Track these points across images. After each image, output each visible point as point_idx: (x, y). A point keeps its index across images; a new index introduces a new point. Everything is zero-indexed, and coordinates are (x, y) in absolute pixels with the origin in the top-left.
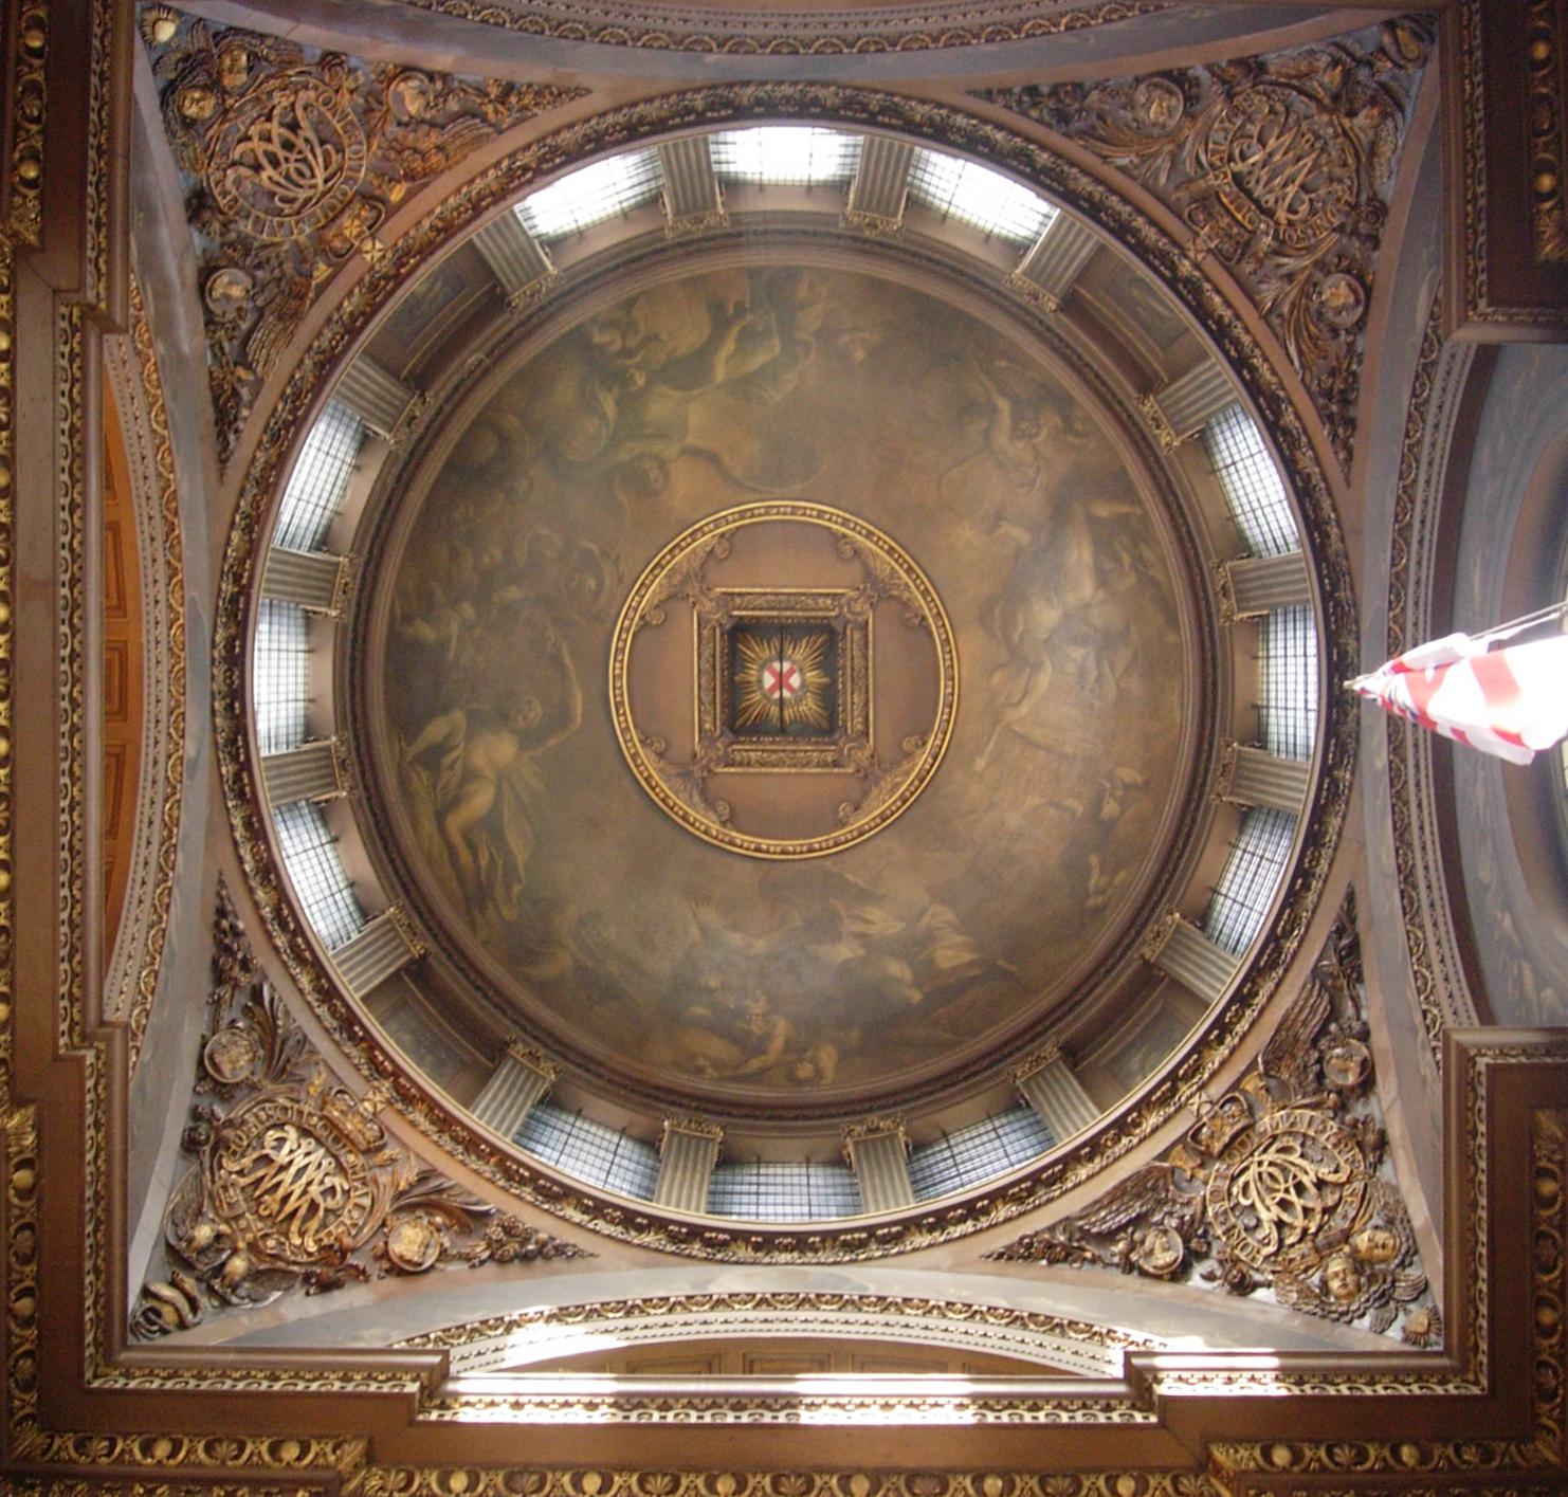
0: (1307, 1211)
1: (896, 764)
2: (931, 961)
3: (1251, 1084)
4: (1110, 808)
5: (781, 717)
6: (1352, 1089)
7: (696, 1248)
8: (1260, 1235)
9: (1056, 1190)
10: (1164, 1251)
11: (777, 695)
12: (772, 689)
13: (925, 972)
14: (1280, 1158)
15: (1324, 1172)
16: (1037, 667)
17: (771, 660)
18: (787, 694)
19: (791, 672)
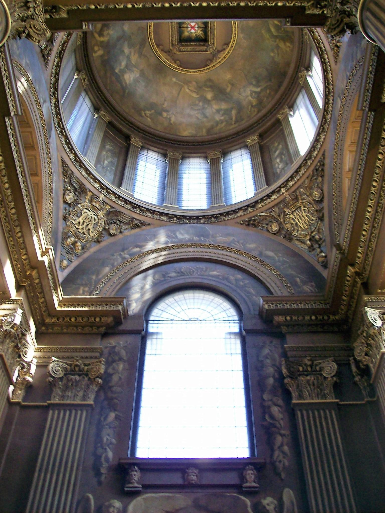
0: (83, 228)
1: (173, 59)
2: (125, 72)
3: (108, 207)
4: (165, 114)
5: (183, 27)
6: (109, 232)
7: (52, 90)
8: (76, 218)
9: (79, 168)
10: (70, 197)
11: (189, 26)
12: (191, 25)
13: (123, 72)
14: (93, 219)
15: (91, 230)
16: (197, 93)
17: (198, 25)
18: (189, 29)
19: (195, 30)
